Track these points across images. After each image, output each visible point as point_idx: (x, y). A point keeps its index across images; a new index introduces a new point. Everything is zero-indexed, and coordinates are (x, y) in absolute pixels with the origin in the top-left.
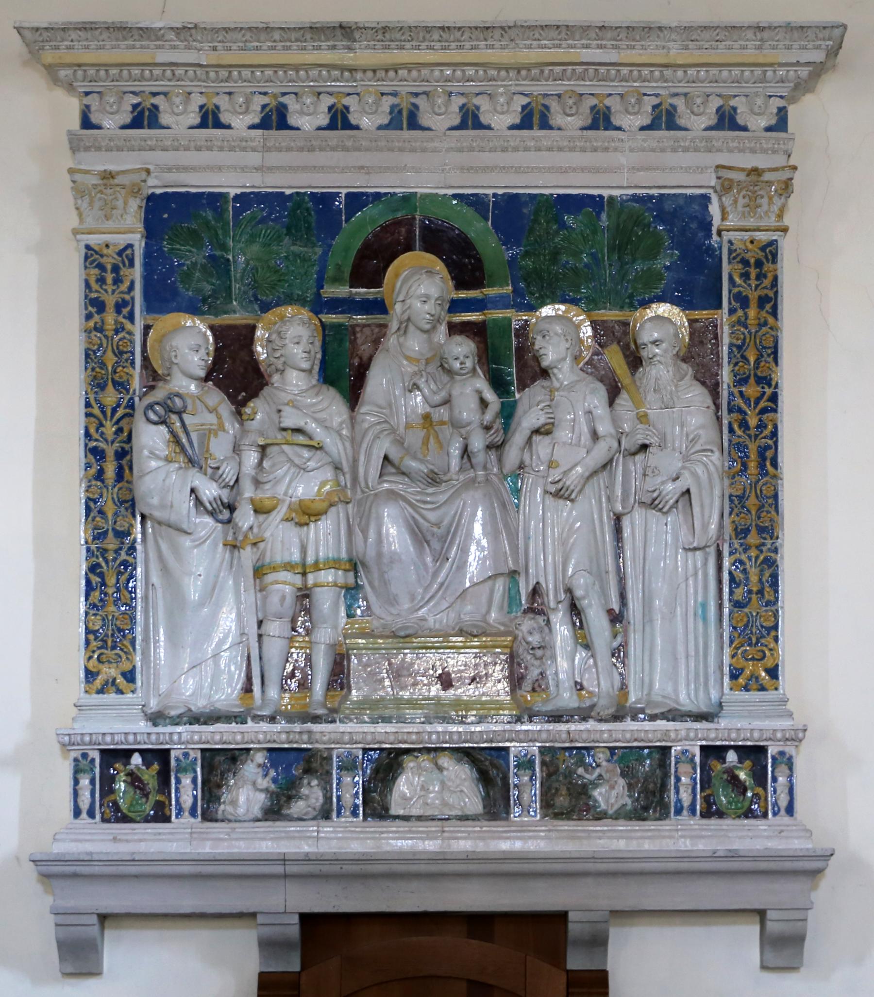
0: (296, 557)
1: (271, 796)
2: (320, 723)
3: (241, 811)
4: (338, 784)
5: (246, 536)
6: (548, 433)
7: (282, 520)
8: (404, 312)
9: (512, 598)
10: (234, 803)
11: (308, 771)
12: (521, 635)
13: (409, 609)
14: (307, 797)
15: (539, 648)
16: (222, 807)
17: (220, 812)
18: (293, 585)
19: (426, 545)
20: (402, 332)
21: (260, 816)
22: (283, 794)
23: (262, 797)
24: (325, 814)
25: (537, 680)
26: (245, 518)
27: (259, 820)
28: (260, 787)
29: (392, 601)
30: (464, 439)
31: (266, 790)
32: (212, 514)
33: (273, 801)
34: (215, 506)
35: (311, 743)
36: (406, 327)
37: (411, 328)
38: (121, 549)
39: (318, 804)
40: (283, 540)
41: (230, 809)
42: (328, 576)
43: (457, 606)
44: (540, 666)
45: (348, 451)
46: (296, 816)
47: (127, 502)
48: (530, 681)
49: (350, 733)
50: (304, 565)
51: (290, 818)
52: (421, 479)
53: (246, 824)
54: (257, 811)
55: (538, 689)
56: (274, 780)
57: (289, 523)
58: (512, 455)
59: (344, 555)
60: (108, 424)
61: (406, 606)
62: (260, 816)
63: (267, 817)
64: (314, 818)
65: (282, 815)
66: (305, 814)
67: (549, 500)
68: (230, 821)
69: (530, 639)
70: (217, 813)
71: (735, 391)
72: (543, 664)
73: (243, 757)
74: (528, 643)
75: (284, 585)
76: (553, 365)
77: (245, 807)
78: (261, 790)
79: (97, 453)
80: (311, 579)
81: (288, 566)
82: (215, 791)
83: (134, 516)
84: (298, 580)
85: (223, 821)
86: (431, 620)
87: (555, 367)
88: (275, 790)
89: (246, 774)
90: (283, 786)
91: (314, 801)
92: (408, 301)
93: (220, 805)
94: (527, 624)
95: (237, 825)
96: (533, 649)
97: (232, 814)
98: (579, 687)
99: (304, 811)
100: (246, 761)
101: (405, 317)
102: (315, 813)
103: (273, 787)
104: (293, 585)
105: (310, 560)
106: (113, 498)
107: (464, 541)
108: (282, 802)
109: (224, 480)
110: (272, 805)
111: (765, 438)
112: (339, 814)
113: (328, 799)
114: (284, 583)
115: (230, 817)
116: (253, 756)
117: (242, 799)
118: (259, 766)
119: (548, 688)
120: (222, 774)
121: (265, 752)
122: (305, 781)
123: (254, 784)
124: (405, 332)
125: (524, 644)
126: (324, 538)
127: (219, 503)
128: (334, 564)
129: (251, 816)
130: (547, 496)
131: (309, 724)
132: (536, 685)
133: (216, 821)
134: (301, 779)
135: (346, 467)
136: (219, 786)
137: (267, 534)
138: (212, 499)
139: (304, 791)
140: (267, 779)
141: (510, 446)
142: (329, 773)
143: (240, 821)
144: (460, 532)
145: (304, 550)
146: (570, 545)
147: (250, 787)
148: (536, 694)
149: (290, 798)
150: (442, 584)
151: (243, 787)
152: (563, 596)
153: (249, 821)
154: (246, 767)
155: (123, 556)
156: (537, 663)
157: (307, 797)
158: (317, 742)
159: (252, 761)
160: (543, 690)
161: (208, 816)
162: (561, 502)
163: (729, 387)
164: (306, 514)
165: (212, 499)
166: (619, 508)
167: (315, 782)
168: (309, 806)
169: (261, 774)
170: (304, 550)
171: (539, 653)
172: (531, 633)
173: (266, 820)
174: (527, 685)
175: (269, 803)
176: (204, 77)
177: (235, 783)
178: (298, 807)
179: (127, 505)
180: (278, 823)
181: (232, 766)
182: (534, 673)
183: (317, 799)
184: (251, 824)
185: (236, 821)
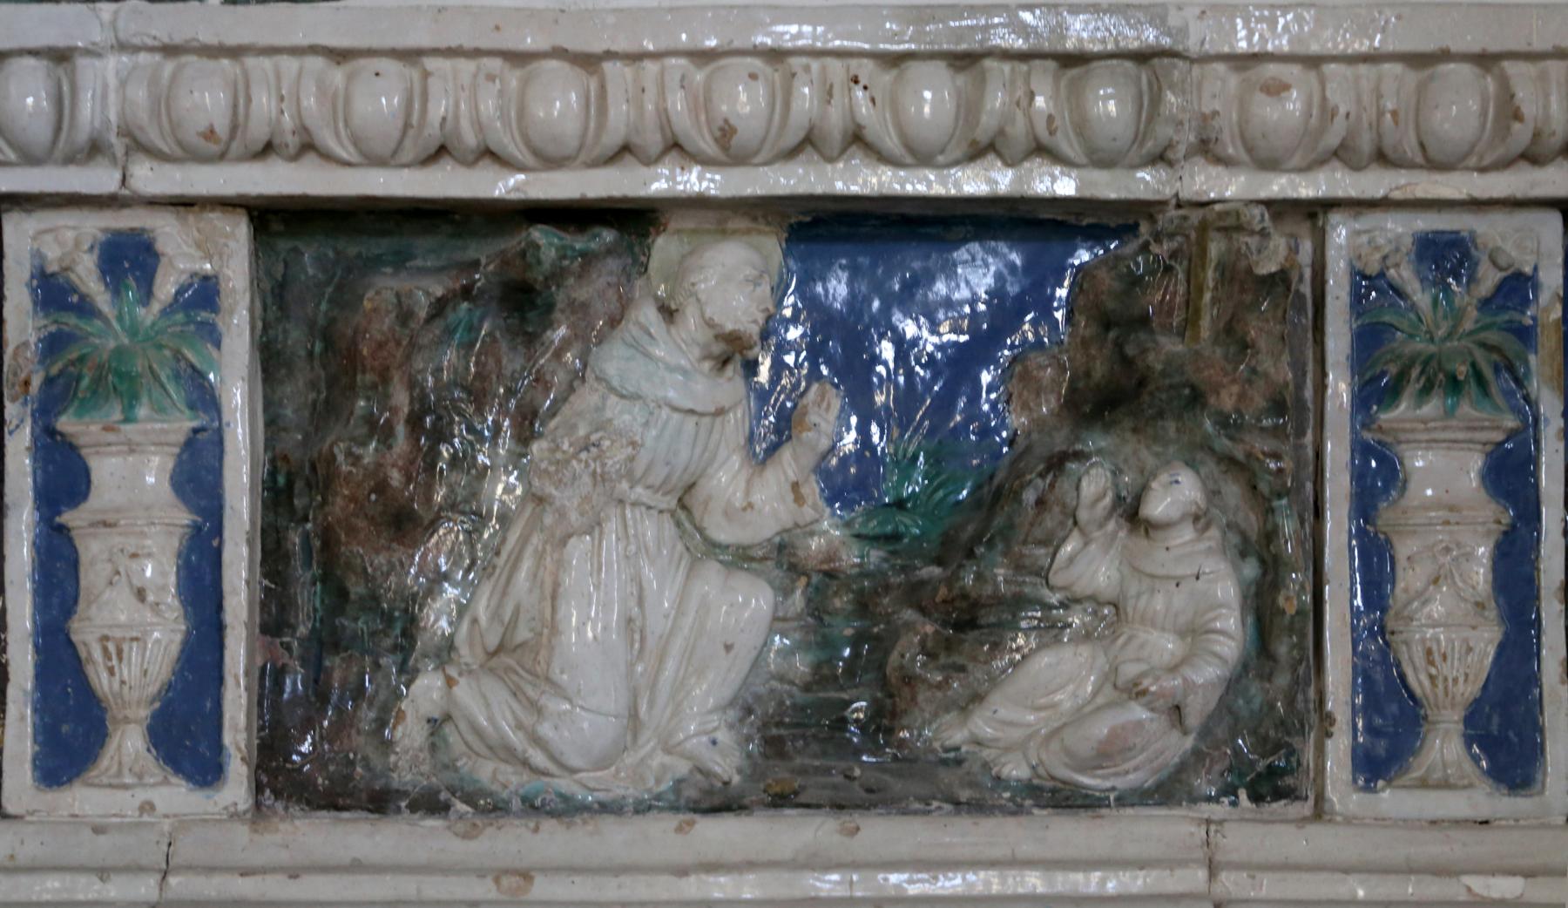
1: (817, 609)
3: (581, 724)
4: (1365, 504)
10: (520, 657)
11: (1117, 395)
14: (1112, 613)
16: (426, 691)
17: (409, 734)
21: (727, 764)
22: (915, 594)
23: (747, 609)
24: (1258, 760)
27: (721, 802)
28: (723, 533)
31: (782, 558)
33: (828, 645)
35: (1160, 158)
39: (1208, 674)
41: (484, 705)
46: (1015, 770)
49: (1485, 60)
51: (970, 791)
53: (616, 838)
54: (704, 733)
56: (847, 484)
62: (727, 764)
63: (781, 775)
64: (1167, 791)
65: (910, 763)
66: (1106, 755)
68: (492, 808)
70: (387, 746)
73: (595, 289)
77: (613, 700)
78: (741, 558)
82: (369, 555)
85: (430, 804)
88: (851, 558)
89: (622, 415)
90: (913, 527)
91: (1168, 646)
93: (409, 673)
95: (552, 841)
97: (508, 754)
99: (1101, 728)
100: (614, 322)
102: (1178, 745)
103: (828, 533)
108: (907, 653)
110: (822, 677)
112: (1374, 767)
113: (1279, 626)
115: (486, 772)
116: (676, 275)
117: (586, 625)
118: (732, 353)
120: (429, 420)
121: (772, 246)
122: (1093, 485)
123: (684, 502)
129: (657, 767)
133: (380, 802)
134: (1056, 463)
136: (404, 524)
139: (1090, 563)
140: (790, 463)
142: (1294, 411)
143: (568, 809)
147: (652, 529)
149: (971, 624)
151: (594, 526)
153: (642, 808)
154: (614, 360)
157: (1112, 613)
158: (1207, 149)
159: (669, 313)
161: (318, 762)
167: (1175, 493)
168: (1135, 691)
169: (736, 424)
173: (781, 800)
175: (801, 665)
177: (538, 500)
178: (1040, 695)
180: (879, 832)
181: (512, 362)
183: (1195, 633)
184: (660, 836)
185: (534, 808)
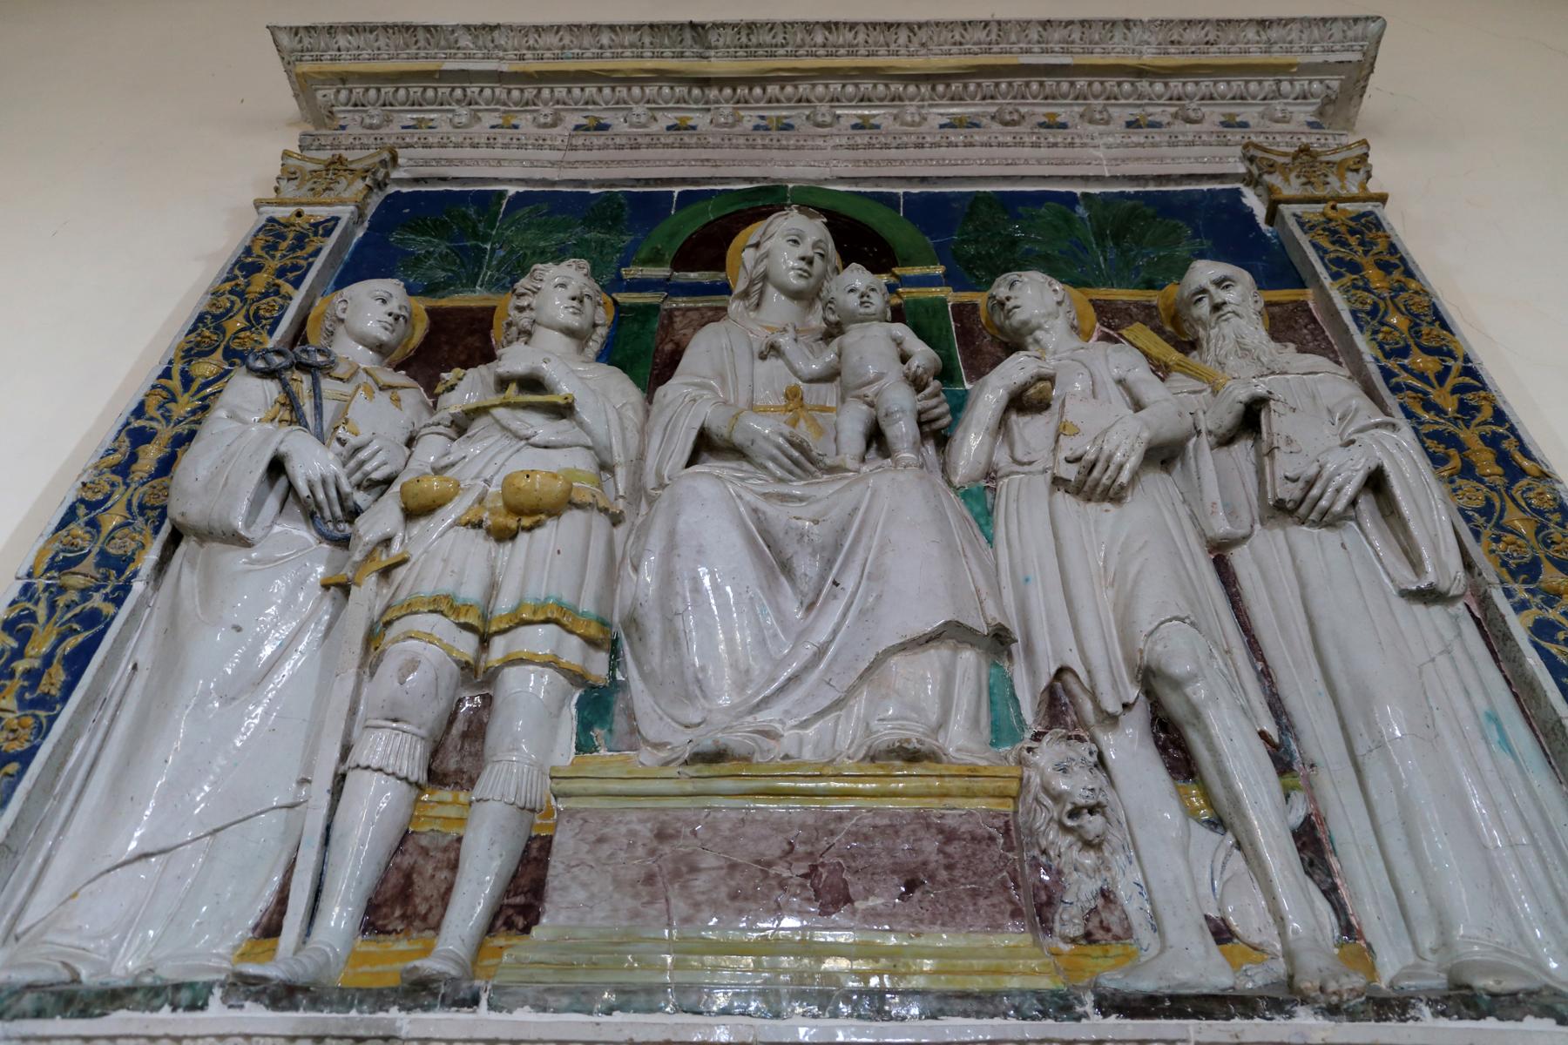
0: (471, 591)
2: (426, 1009)
5: (370, 556)
6: (1042, 406)
7: (457, 523)
8: (757, 262)
9: (999, 696)
12: (1036, 780)
13: (733, 707)
15: (1091, 811)
18: (448, 650)
19: (783, 579)
20: (754, 300)
25: (1094, 910)
26: (381, 519)
29: (691, 687)
30: (871, 405)
32: (311, 514)
34: (321, 496)
36: (762, 293)
37: (770, 289)
38: (97, 589)
40: (447, 557)
42: (539, 639)
43: (859, 706)
44: (1097, 870)
45: (629, 435)
47: (153, 508)
48: (1075, 910)
50: (485, 618)
52: (775, 452)
55: (1099, 934)
57: (472, 532)
58: (972, 444)
59: (587, 605)
60: (184, 398)
61: (724, 701)
67: (1067, 503)
69: (1063, 785)
71: (1391, 364)
72: (1104, 865)
74: (1057, 798)
75: (427, 653)
76: (1034, 322)
79: (140, 437)
80: (499, 648)
81: (443, 605)
83: (156, 531)
84: (467, 645)
86: (789, 735)
87: (1039, 327)
92: (766, 246)
94: (1048, 753)
96: (1075, 813)
98: (1222, 933)
101: (761, 268)
104: (448, 650)
105: (504, 604)
106: (129, 503)
107: (876, 558)
109: (362, 464)
111: (1485, 423)
114: (429, 638)
119: (1129, 931)
124: (758, 305)
125: (1048, 802)
126: (548, 563)
127: (333, 494)
128: (558, 617)
130: (1060, 495)
131: (394, 1012)
132: (1095, 921)
135: (618, 456)
137: (416, 553)
138: (316, 478)
141: (966, 431)
144: (865, 540)
145: (493, 588)
146: (1131, 576)
148: (1094, 950)
150: (821, 652)
152: (1133, 692)
155: (97, 601)
156: (1089, 859)
160: (1117, 938)
162: (1092, 508)
163: (1377, 360)
164: (519, 515)
165: (316, 478)
166: (1221, 526)
170: (493, 588)
171: (1093, 824)
172: (1064, 770)
174: (1069, 921)
176: (504, 96)
179: (150, 513)
182: (1081, 890)
